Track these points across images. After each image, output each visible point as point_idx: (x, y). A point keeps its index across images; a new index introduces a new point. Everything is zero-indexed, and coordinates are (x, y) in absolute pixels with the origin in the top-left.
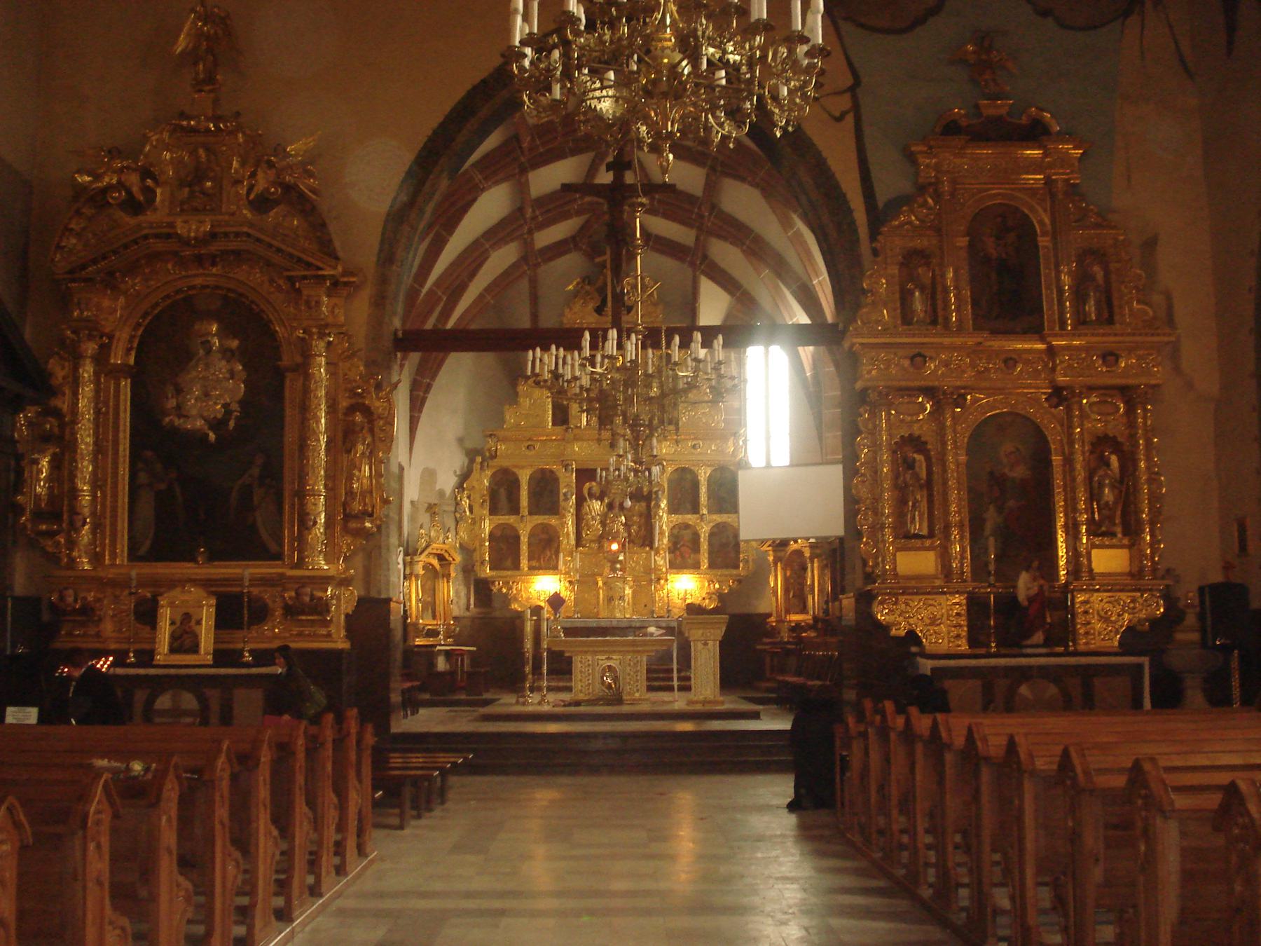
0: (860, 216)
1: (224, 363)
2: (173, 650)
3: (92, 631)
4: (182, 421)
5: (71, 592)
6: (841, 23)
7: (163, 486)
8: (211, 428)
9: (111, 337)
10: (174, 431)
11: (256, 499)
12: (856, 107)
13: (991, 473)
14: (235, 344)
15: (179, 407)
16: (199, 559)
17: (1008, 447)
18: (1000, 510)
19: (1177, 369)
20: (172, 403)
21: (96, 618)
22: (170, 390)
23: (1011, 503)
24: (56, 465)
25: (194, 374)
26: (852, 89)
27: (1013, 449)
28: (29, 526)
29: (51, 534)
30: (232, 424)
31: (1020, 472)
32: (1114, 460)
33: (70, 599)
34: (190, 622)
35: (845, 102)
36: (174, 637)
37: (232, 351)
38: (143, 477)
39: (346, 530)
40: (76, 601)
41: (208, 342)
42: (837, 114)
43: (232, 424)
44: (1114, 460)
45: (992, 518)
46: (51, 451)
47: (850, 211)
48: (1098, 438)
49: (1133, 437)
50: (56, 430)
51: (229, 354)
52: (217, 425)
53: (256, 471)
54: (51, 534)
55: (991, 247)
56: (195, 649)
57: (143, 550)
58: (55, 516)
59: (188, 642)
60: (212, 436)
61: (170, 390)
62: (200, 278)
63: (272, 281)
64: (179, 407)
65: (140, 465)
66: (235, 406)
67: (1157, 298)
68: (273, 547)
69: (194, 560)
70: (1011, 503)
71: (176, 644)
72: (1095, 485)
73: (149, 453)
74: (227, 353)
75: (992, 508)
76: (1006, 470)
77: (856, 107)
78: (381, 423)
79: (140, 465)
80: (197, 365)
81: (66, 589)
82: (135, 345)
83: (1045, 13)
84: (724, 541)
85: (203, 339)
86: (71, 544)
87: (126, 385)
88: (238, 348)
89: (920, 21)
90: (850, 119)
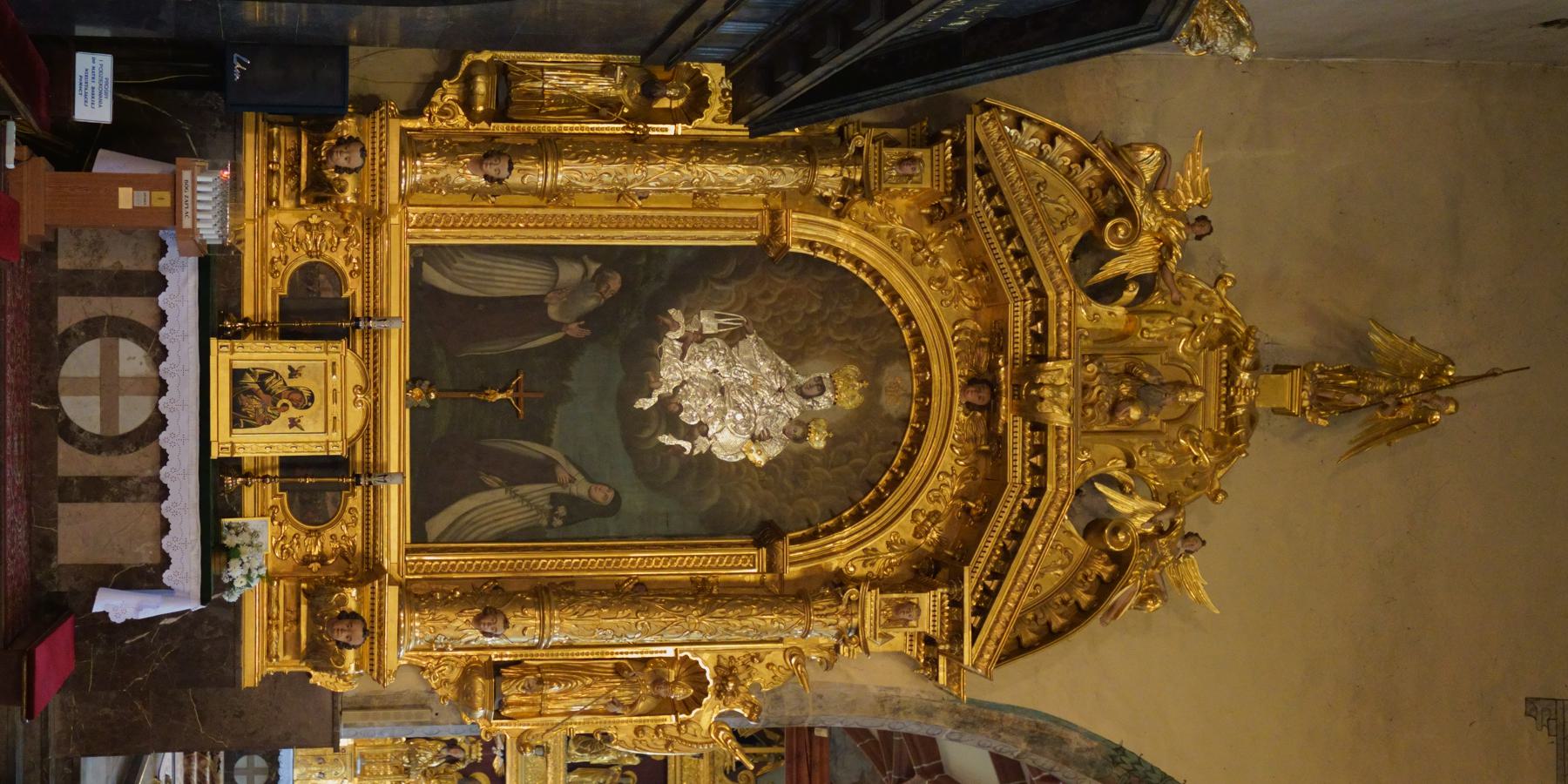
1: (782, 422)
3: (282, 189)
5: (356, 161)
7: (553, 312)
8: (663, 400)
14: (818, 441)
15: (701, 338)
16: (417, 392)
20: (708, 323)
21: (303, 201)
22: (733, 320)
24: (601, 108)
29: (467, 103)
30: (668, 440)
33: (341, 160)
34: (296, 406)
36: (264, 377)
38: (570, 272)
39: (468, 673)
40: (339, 169)
41: (822, 390)
43: (668, 440)
50: (664, 103)
51: (799, 431)
52: (667, 412)
53: (581, 488)
54: (467, 103)
57: (431, 275)
60: (645, 404)
61: (733, 320)
63: (934, 516)
64: (701, 338)
66: (702, 445)
68: (438, 524)
71: (250, 381)
73: (615, 283)
74: (799, 429)
80: (778, 371)
81: (363, 152)
82: (821, 255)
85: (827, 383)
87: (746, 239)
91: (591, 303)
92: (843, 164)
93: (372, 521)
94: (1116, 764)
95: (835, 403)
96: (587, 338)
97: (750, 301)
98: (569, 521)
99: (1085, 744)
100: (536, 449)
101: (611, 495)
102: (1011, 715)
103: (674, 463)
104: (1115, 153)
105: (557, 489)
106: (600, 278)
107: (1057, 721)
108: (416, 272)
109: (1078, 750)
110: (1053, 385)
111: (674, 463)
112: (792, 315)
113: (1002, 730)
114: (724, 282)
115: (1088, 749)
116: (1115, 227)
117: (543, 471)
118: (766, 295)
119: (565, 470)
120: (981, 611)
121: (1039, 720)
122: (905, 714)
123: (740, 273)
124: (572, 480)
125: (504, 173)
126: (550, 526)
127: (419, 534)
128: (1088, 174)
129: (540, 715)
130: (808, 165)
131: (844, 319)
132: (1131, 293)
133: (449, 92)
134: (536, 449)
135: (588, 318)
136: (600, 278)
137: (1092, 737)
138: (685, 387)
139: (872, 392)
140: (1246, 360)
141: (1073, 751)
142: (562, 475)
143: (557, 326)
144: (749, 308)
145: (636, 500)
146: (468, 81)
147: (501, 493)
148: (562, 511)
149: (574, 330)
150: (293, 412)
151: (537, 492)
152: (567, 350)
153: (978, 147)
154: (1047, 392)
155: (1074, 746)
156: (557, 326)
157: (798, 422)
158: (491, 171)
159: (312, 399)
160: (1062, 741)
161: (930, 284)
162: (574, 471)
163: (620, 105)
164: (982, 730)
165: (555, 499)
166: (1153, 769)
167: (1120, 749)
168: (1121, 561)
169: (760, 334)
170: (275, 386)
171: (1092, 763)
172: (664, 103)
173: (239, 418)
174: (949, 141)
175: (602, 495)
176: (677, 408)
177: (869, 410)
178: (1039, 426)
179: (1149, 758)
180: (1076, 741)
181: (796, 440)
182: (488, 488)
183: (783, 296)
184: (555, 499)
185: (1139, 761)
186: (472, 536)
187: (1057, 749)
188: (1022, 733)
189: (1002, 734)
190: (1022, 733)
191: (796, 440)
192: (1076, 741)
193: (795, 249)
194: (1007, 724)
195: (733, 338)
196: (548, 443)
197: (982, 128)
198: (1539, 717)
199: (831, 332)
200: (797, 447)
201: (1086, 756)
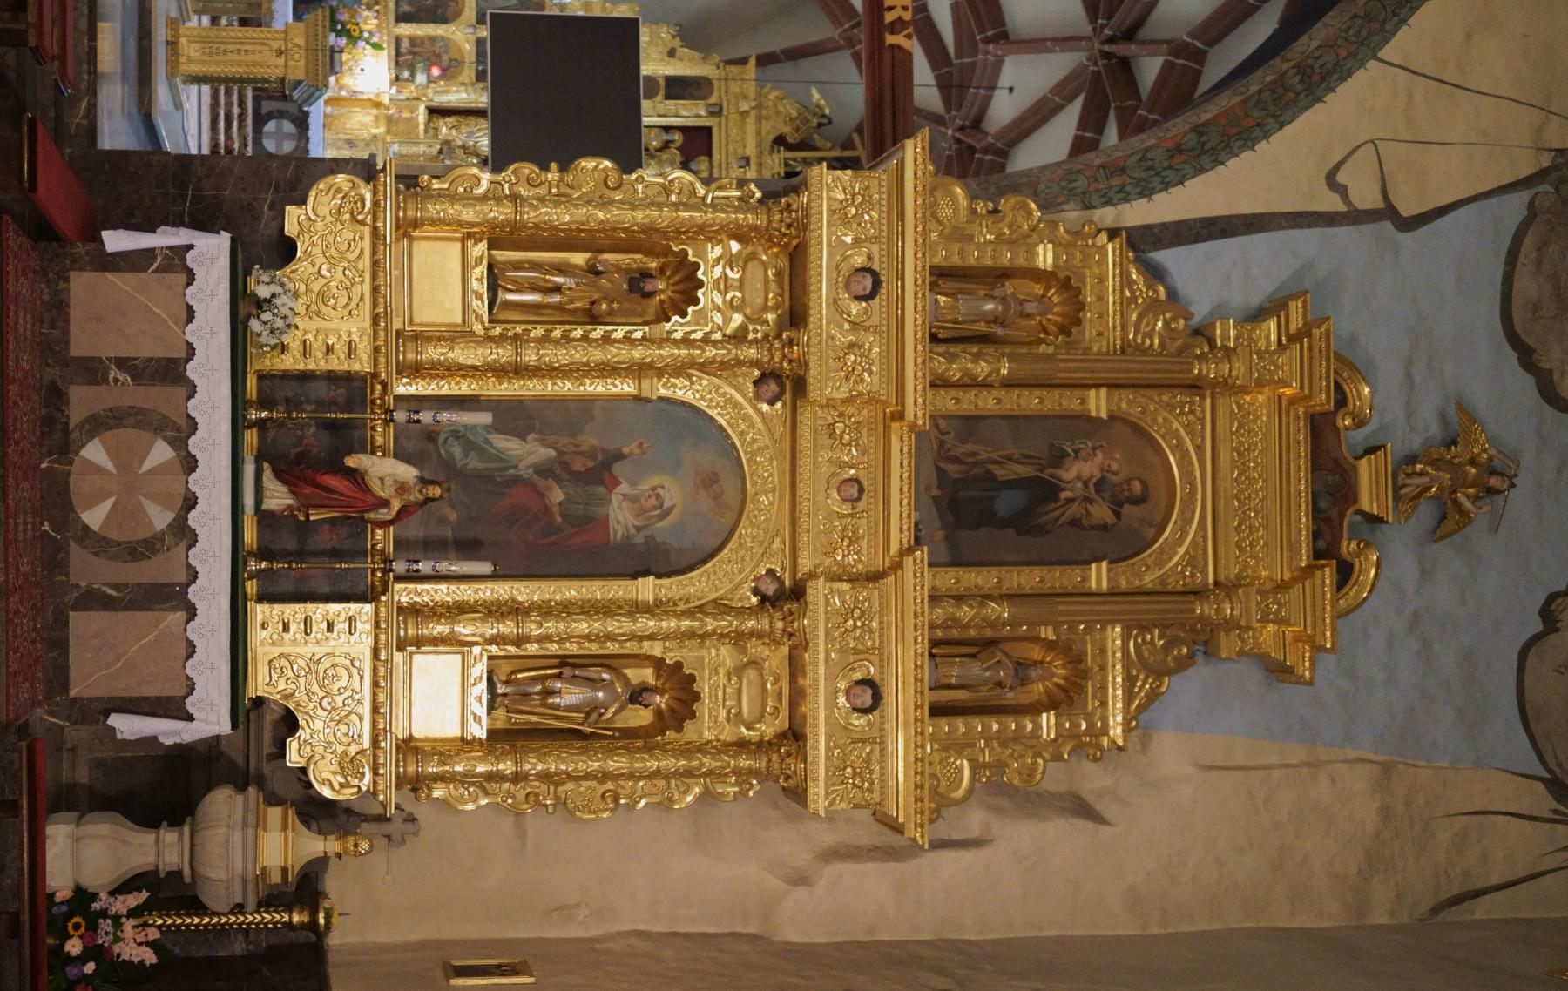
0: (1138, 213)
6: (1524, 196)
12: (1354, 217)
13: (620, 456)
17: (673, 494)
18: (543, 470)
19: (835, 854)
23: (557, 495)
26: (1389, 212)
27: (667, 504)
31: (620, 516)
32: (641, 717)
35: (1366, 196)
42: (1341, 177)
44: (641, 717)
45: (526, 452)
47: (1147, 192)
48: (692, 678)
49: (689, 750)
55: (1079, 471)
67: (975, 820)
70: (557, 495)
72: (592, 672)
75: (545, 453)
76: (624, 488)
77: (1354, 217)
83: (1548, 614)
89: (1527, 357)
90: (1332, 203)
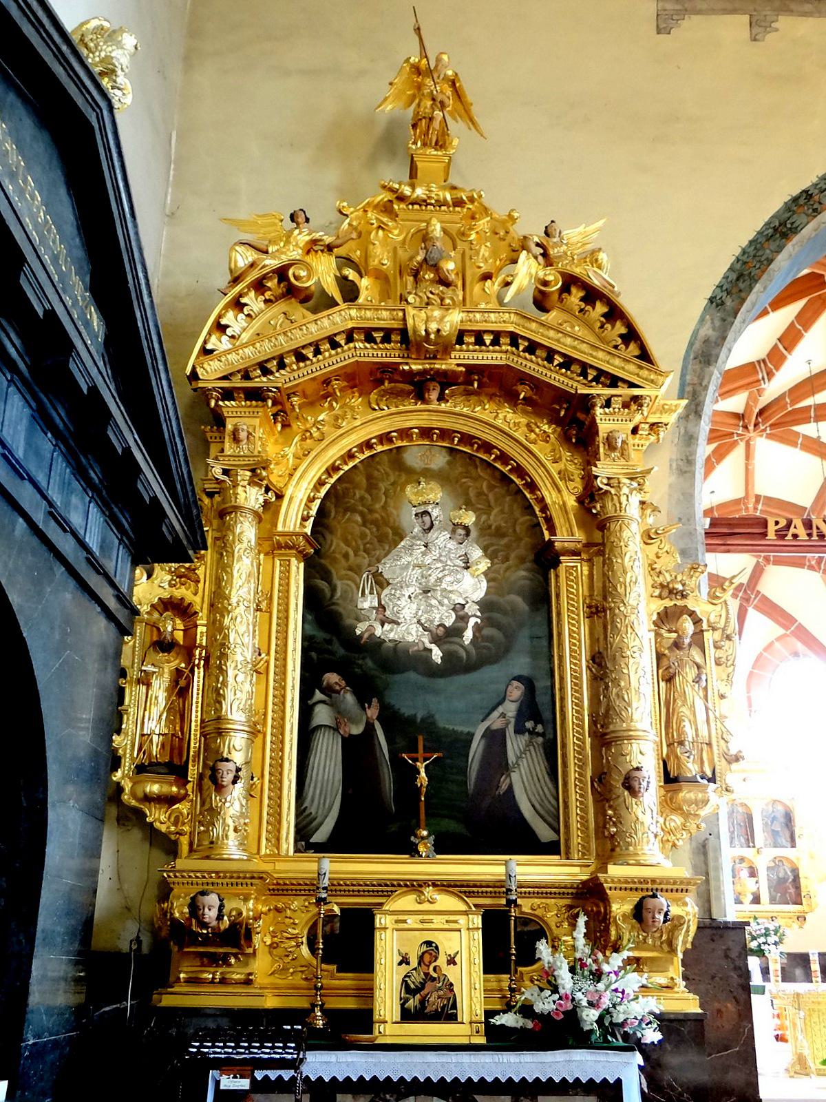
1: (452, 545)
2: (407, 1016)
4: (387, 627)
5: (213, 899)
7: (357, 730)
8: (436, 640)
9: (280, 497)
10: (375, 645)
11: (511, 757)
14: (469, 518)
15: (382, 607)
16: (421, 848)
21: (250, 950)
24: (180, 688)
25: (406, 559)
28: (127, 785)
29: (169, 800)
30: (468, 635)
34: (436, 958)
36: (408, 989)
37: (467, 530)
38: (322, 715)
40: (220, 917)
41: (426, 513)
43: (468, 635)
46: (174, 665)
50: (179, 636)
51: (461, 531)
53: (510, 709)
56: (448, 1014)
57: (320, 836)
58: (178, 771)
59: (434, 1003)
60: (437, 655)
62: (413, 415)
65: (318, 695)
66: (472, 609)
68: (544, 833)
69: (412, 851)
71: (412, 1003)
73: (332, 678)
74: (461, 532)
78: (717, 636)
79: (318, 695)
81: (203, 893)
82: (313, 512)
84: (781, 875)
85: (422, 509)
86: (210, 814)
87: (297, 571)
88: (476, 524)
91: (349, 698)
92: (235, 486)
93: (541, 890)
94: (723, 303)
95: (437, 504)
96: (381, 702)
97: (350, 569)
98: (538, 719)
99: (708, 324)
100: (477, 747)
101: (515, 683)
102: (688, 377)
103: (487, 631)
104: (236, 280)
105: (511, 728)
106: (329, 690)
107: (691, 344)
108: (320, 848)
109: (714, 329)
110: (427, 322)
111: (487, 631)
112: (363, 536)
113: (701, 384)
114: (333, 590)
115: (712, 322)
116: (296, 278)
117: (496, 739)
118: (346, 556)
119: (495, 722)
120: (614, 381)
121: (692, 357)
122: (691, 455)
123: (326, 576)
124: (503, 715)
125: (231, 766)
126: (543, 735)
127: (551, 848)
128: (253, 302)
129: (709, 744)
130: (236, 513)
131: (367, 496)
132: (351, 274)
133: (158, 817)
134: (477, 747)
135: (363, 700)
136: (329, 690)
137: (702, 320)
138: (423, 622)
139: (428, 474)
140: (407, 191)
141: (714, 333)
142: (498, 725)
143: (370, 727)
144: (357, 570)
145: (520, 663)
146: (148, 799)
147: (515, 776)
148: (529, 725)
149: (373, 712)
150: (442, 961)
151: (515, 745)
152: (390, 718)
153: (225, 378)
154: (433, 327)
155: (710, 332)
156: (370, 727)
157: (453, 532)
158: (228, 778)
159: (429, 943)
160: (707, 341)
161: (340, 427)
162: (496, 714)
163: (178, 673)
164: (701, 398)
165: (519, 730)
166: (725, 277)
167: (711, 300)
168: (570, 281)
169: (379, 561)
170: (417, 978)
171: (724, 320)
172: (179, 636)
173: (448, 1014)
174: (221, 403)
175: (516, 691)
176: (441, 628)
177: (441, 477)
178: (460, 337)
179: (717, 279)
180: (707, 331)
181: (468, 533)
182: (510, 787)
183: (348, 544)
184: (519, 730)
185: (720, 286)
186: (553, 802)
187: (713, 344)
188: (702, 369)
189: (704, 384)
190: (703, 371)
191: (468, 533)
192: (707, 331)
193: (308, 530)
194: (696, 380)
195: (381, 582)
196: (472, 735)
197: (211, 372)
198: (671, 26)
199: (377, 506)
200: (474, 534)
201: (717, 323)
